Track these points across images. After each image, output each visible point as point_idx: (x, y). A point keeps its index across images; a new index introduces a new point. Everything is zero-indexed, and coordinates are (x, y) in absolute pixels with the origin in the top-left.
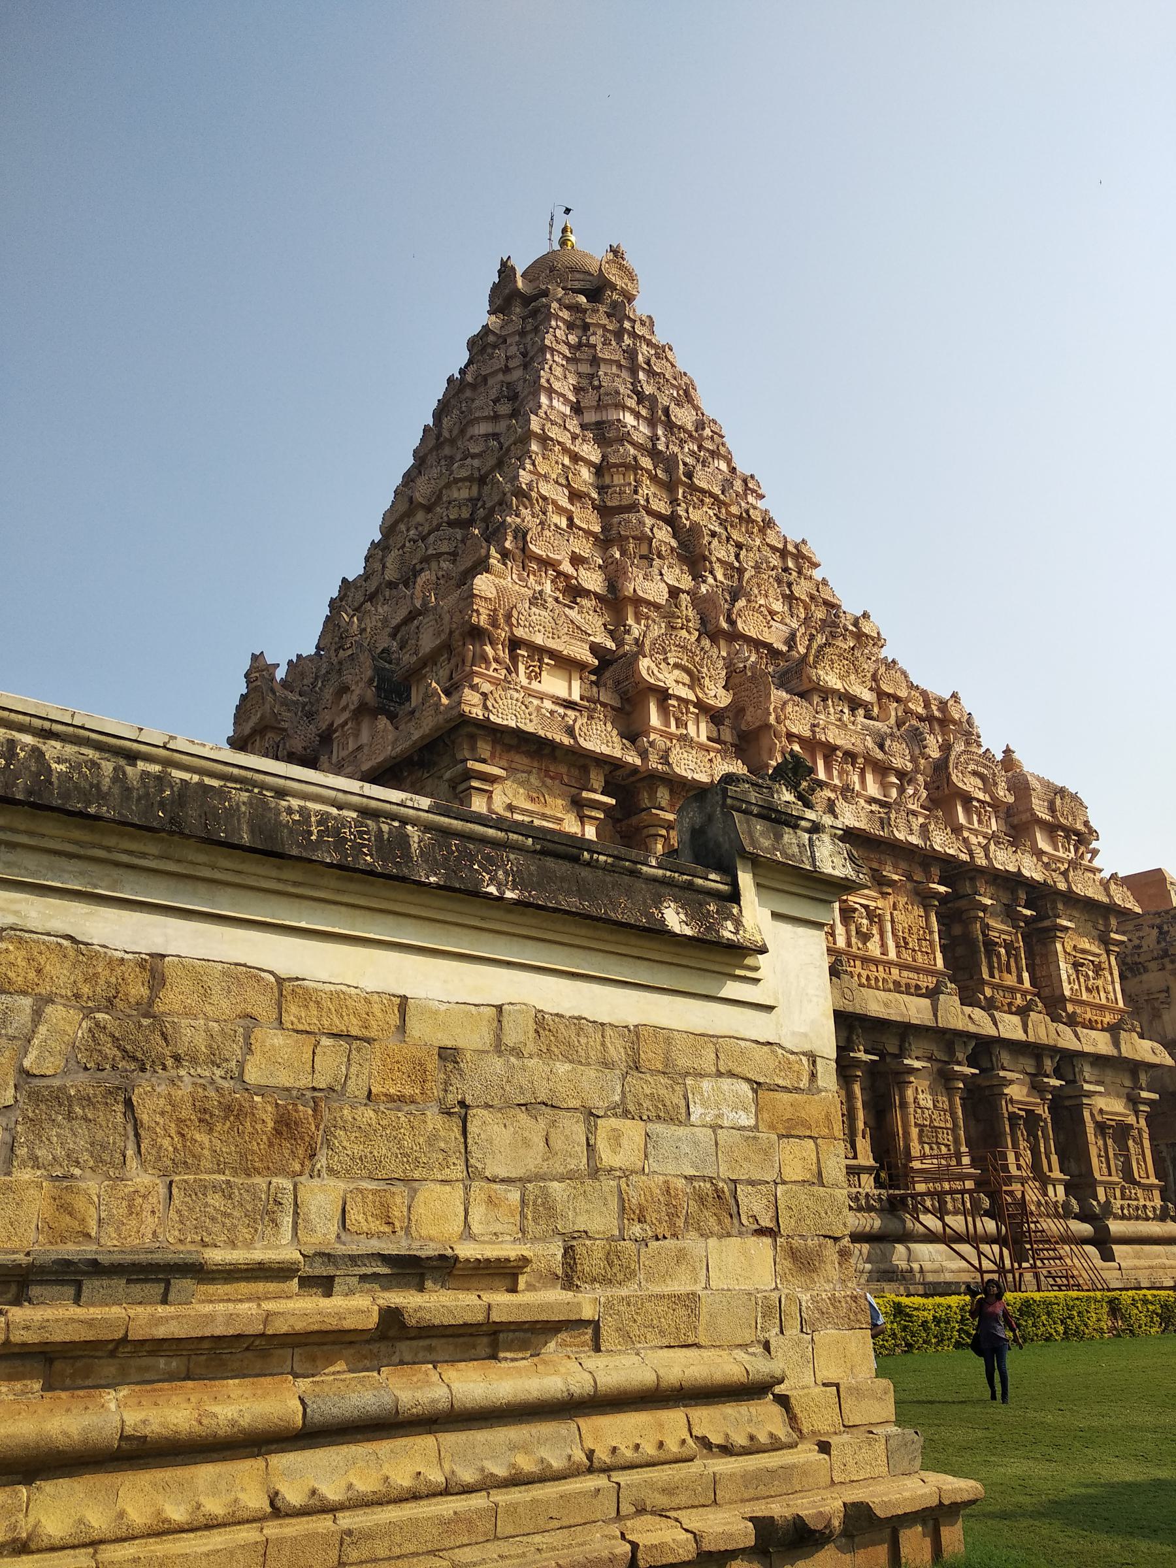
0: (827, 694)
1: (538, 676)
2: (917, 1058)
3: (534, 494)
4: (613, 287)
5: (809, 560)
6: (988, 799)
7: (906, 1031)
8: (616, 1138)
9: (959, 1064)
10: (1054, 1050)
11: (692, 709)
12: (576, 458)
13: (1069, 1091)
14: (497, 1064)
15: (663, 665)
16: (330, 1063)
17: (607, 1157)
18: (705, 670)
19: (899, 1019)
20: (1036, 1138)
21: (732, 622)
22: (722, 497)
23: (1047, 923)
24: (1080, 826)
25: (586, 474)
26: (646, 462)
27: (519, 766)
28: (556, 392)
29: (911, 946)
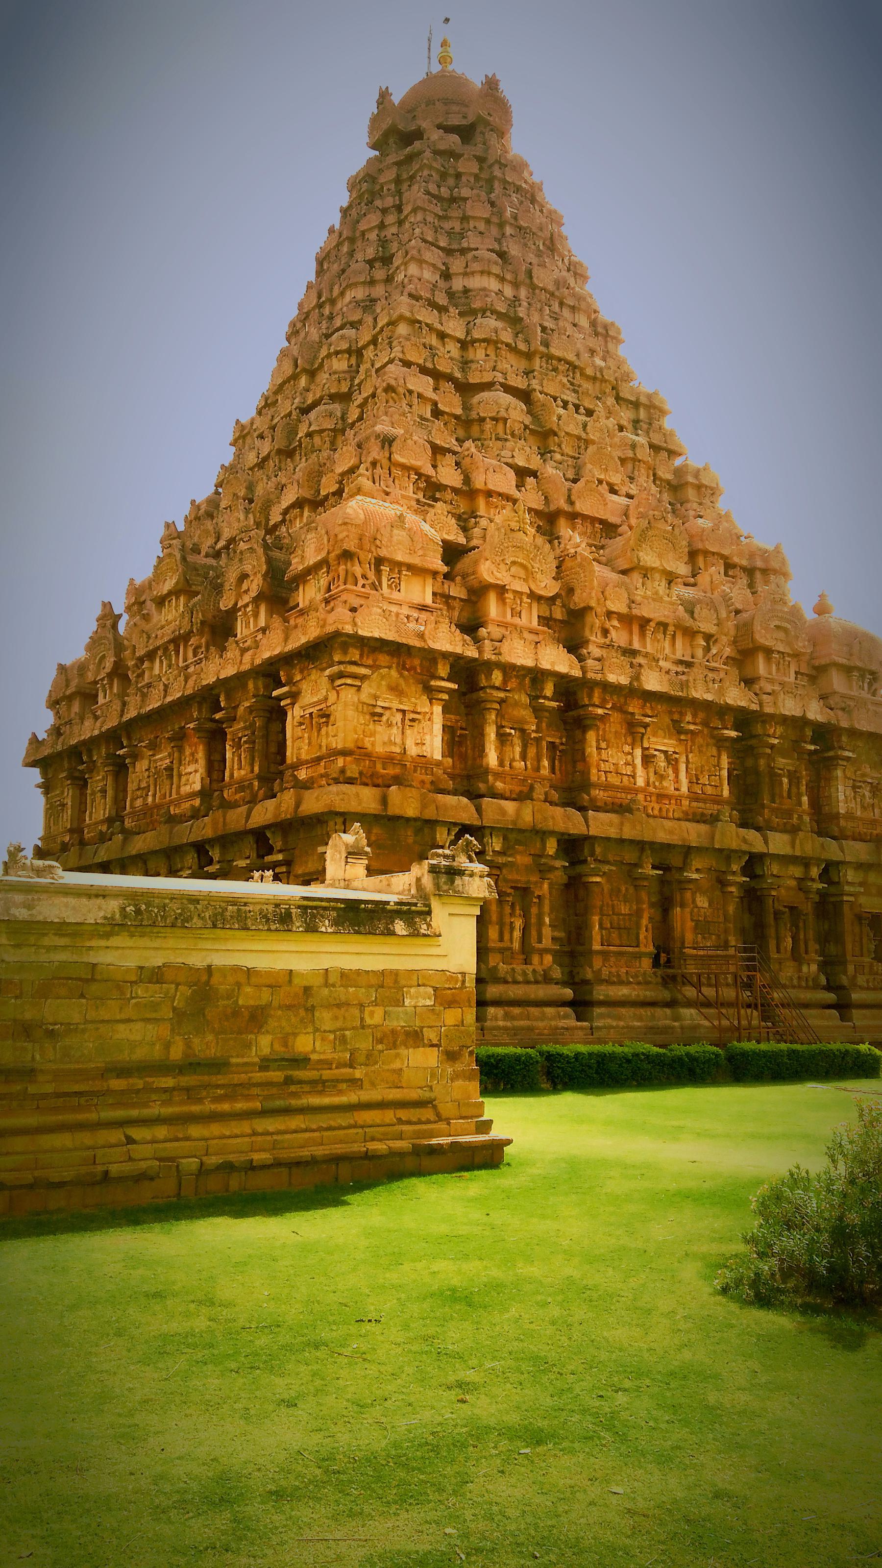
0: (646, 573)
3: (401, 390)
8: (372, 1014)
13: (833, 890)
14: (326, 991)
15: (502, 566)
16: (265, 996)
17: (369, 1021)
20: (797, 927)
23: (831, 754)
25: (453, 349)
28: (426, 262)
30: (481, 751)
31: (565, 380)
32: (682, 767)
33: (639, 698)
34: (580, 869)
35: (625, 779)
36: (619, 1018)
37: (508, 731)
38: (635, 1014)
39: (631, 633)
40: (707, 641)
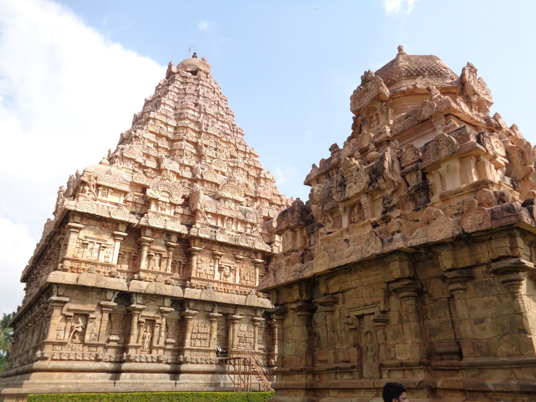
0: (226, 199)
2: (240, 315)
3: (140, 137)
4: (201, 70)
5: (254, 154)
7: (236, 307)
9: (259, 317)
11: (168, 205)
12: (166, 125)
15: (157, 191)
18: (175, 192)
19: (230, 303)
21: (202, 176)
22: (218, 136)
25: (171, 130)
26: (192, 126)
29: (246, 279)
31: (213, 141)
32: (238, 273)
34: (183, 313)
35: (209, 276)
36: (193, 379)
37: (151, 254)
38: (202, 377)
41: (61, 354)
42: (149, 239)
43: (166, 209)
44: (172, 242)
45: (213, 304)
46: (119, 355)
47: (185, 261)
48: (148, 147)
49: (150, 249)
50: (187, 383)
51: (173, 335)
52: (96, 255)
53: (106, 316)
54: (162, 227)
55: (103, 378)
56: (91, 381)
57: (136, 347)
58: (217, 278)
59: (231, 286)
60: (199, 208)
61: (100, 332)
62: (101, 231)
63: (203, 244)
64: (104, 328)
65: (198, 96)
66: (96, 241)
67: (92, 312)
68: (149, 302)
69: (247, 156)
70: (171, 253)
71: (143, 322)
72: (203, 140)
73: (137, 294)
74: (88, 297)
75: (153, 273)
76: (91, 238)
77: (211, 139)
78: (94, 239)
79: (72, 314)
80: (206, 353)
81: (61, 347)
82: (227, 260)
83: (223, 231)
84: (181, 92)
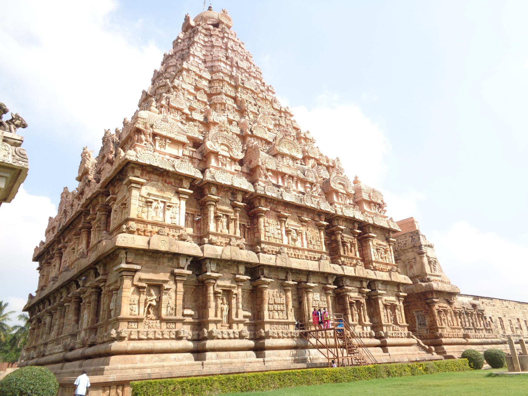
0: (283, 155)
1: (164, 147)
2: (313, 283)
3: (180, 88)
4: (223, 23)
5: (289, 113)
6: (345, 192)
7: (309, 273)
9: (330, 284)
10: (366, 279)
11: (228, 159)
12: (201, 77)
13: (373, 293)
15: (216, 144)
18: (234, 146)
19: (304, 269)
20: (360, 310)
21: (252, 132)
22: (255, 91)
23: (366, 235)
24: (379, 202)
25: (205, 83)
26: (227, 79)
27: (154, 179)
28: (196, 56)
29: (313, 243)
30: (207, 224)
32: (304, 236)
33: (282, 206)
34: (258, 282)
35: (278, 240)
36: (279, 356)
37: (220, 215)
38: (287, 353)
39: (278, 179)
40: (311, 186)
41: (139, 332)
42: (216, 197)
43: (227, 165)
44: (238, 201)
45: (287, 270)
46: (197, 332)
47: (249, 224)
48: (188, 99)
49: (217, 209)
50: (275, 361)
51: (247, 307)
52: (161, 215)
53: (180, 286)
54: (229, 183)
55: (188, 359)
56: (178, 363)
57: (216, 322)
58: (285, 242)
59: (300, 251)
60: (260, 164)
61: (176, 305)
62: (164, 188)
63: (268, 204)
64: (180, 302)
65: (226, 49)
66: (160, 199)
67: (166, 282)
68: (223, 270)
69: (283, 115)
70: (238, 214)
71: (220, 293)
72: (242, 95)
73: (211, 259)
74: (159, 264)
75: (223, 236)
76: (154, 195)
77: (248, 95)
78: (157, 196)
79: (144, 285)
80: (285, 326)
81: (136, 324)
82: (293, 223)
83: (287, 189)
84: (207, 44)
